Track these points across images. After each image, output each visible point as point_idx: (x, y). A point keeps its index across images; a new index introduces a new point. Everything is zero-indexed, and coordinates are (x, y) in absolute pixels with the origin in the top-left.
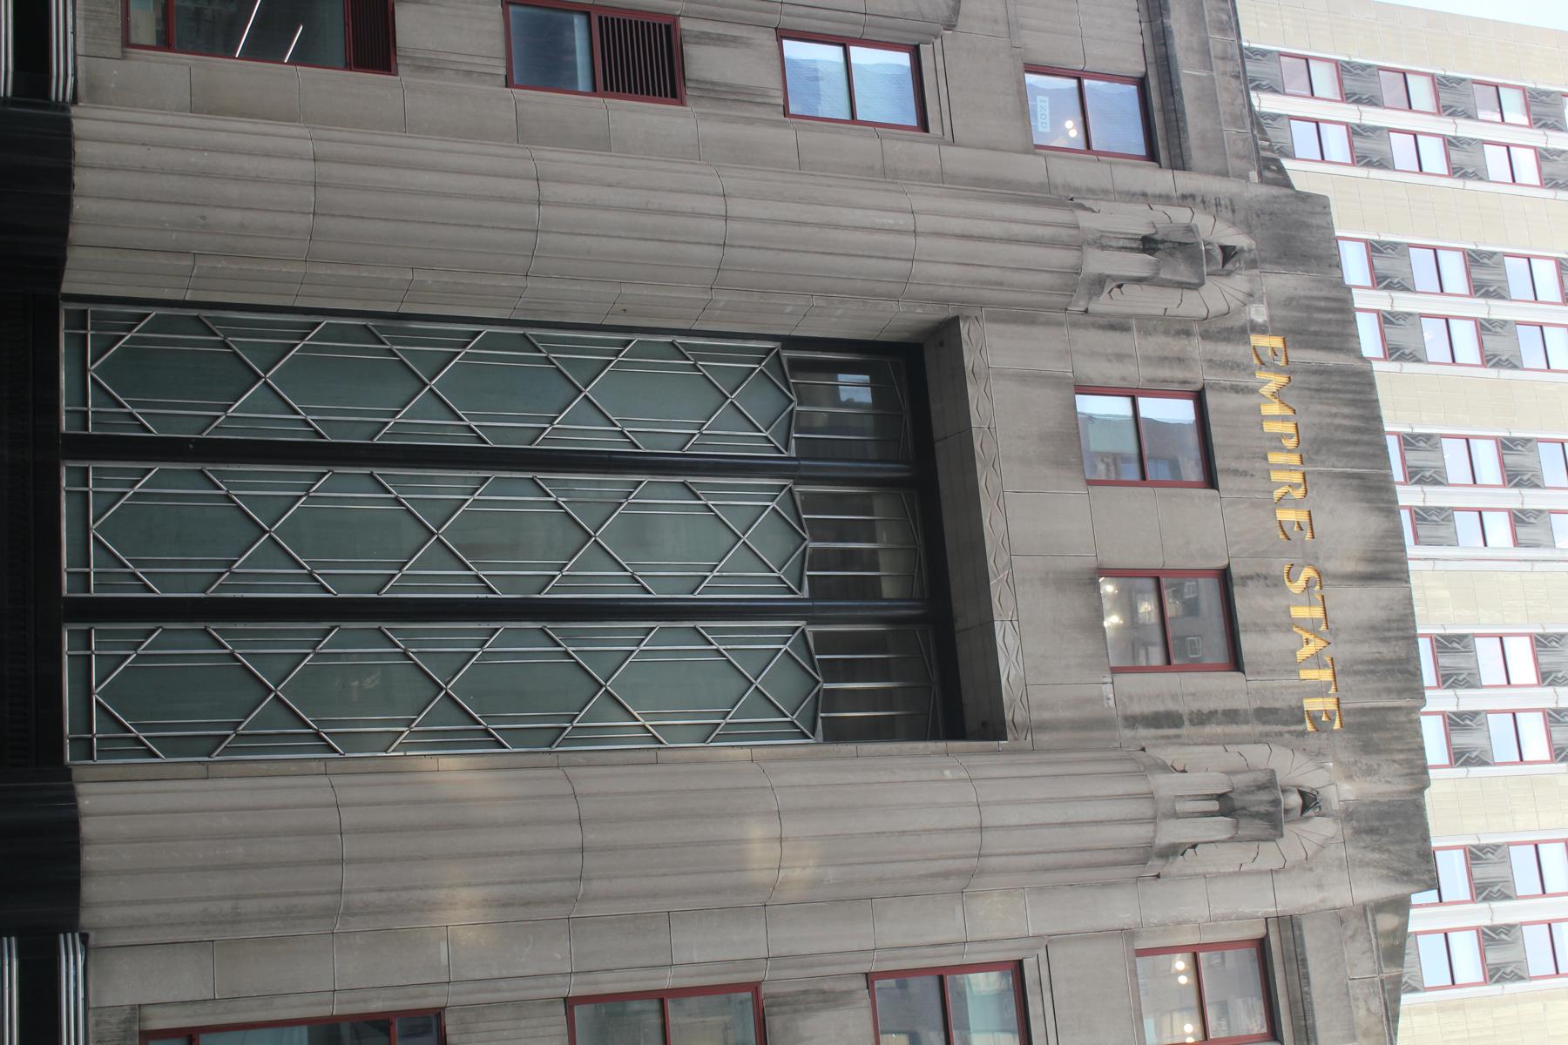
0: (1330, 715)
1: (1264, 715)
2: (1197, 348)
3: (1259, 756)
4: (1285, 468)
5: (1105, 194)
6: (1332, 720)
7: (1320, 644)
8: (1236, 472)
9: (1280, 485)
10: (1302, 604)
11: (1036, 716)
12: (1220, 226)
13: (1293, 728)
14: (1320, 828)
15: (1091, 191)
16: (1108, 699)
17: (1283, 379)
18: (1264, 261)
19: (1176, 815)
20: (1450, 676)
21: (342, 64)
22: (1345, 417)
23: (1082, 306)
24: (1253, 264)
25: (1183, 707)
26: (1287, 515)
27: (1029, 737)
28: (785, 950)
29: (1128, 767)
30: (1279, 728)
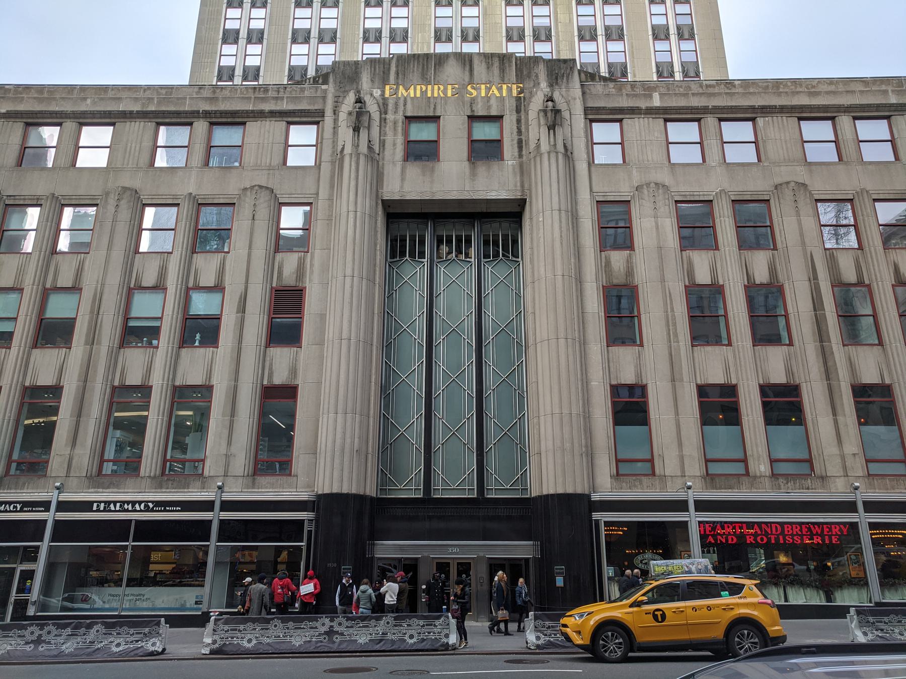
0: (518, 87)
1: (518, 111)
2: (390, 117)
3: (532, 115)
4: (435, 91)
5: (335, 142)
6: (520, 87)
7: (494, 87)
8: (435, 109)
9: (438, 93)
10: (481, 92)
11: (519, 188)
12: (346, 102)
13: (522, 101)
14: (556, 96)
15: (333, 147)
17: (401, 87)
18: (357, 88)
19: (555, 145)
20: (449, 38)
21: (289, 402)
22: (414, 67)
23: (376, 155)
24: (359, 92)
25: (516, 138)
26: (449, 94)
28: (594, 277)
29: (538, 159)
30: (523, 107)
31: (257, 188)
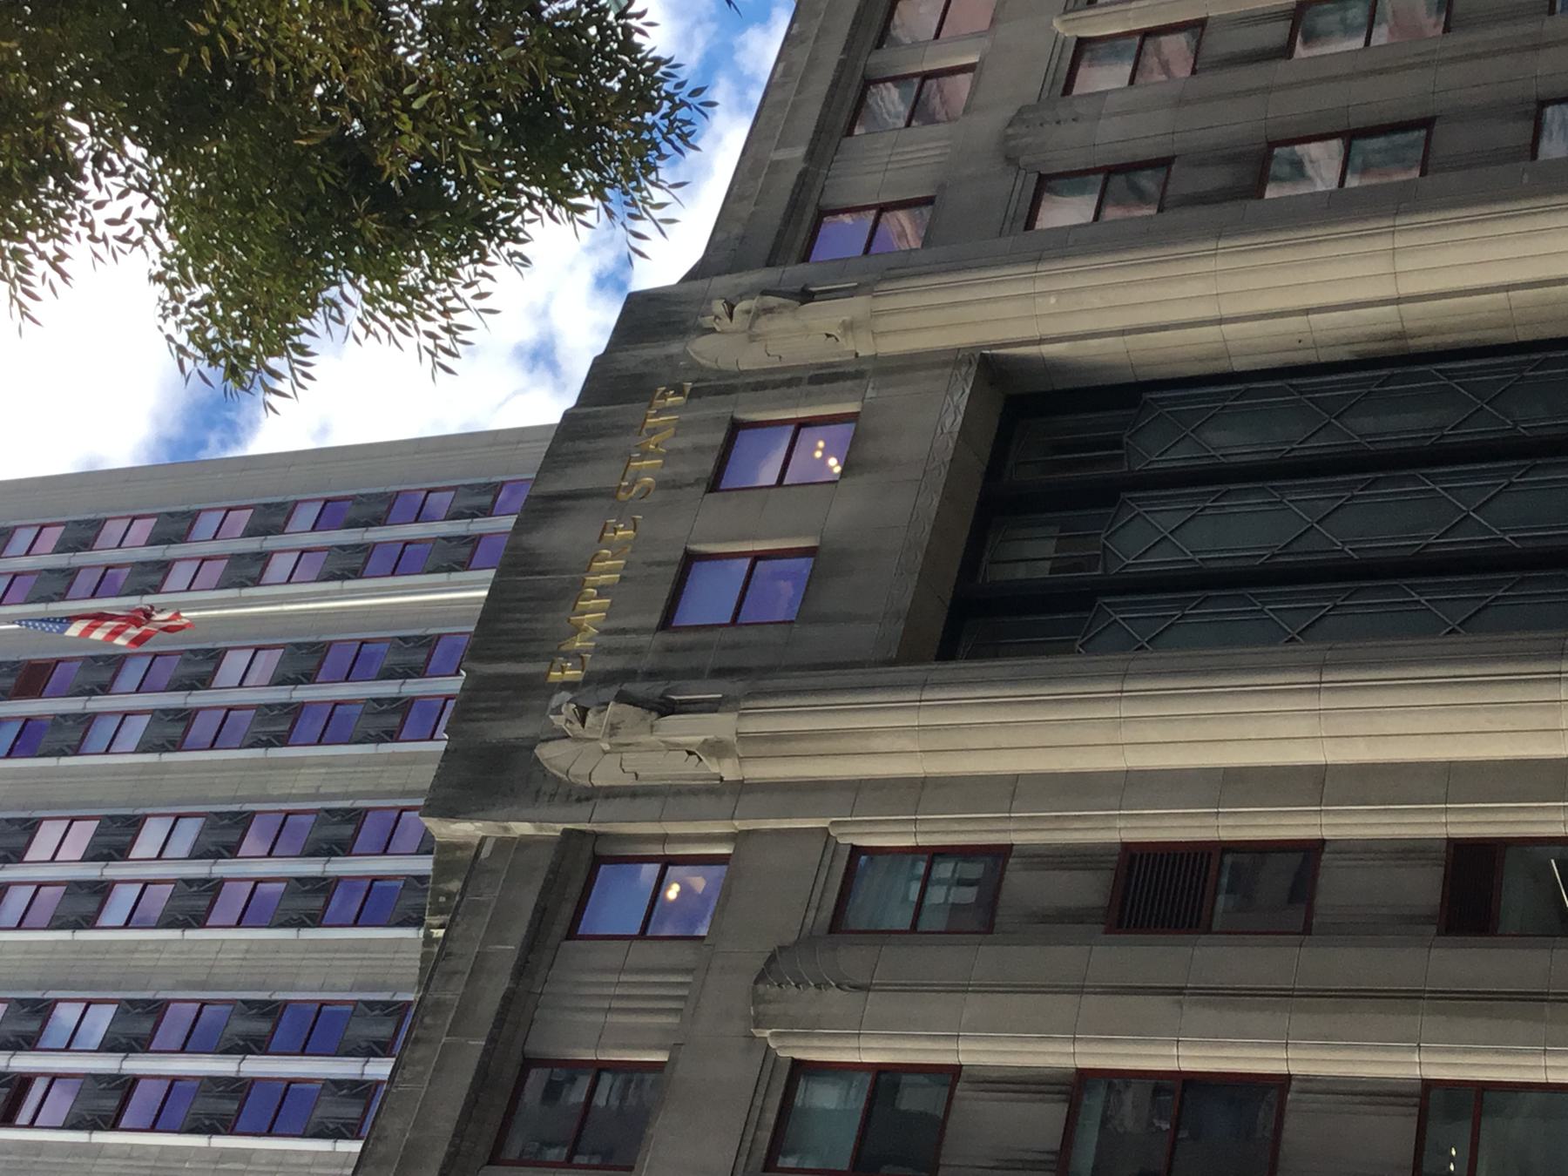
1: (729, 390)
4: (607, 570)
16: (873, 388)
22: (518, 620)
27: (960, 356)
31: (761, 987)
